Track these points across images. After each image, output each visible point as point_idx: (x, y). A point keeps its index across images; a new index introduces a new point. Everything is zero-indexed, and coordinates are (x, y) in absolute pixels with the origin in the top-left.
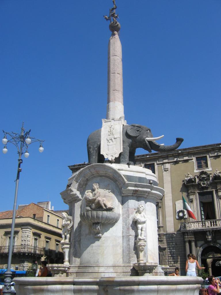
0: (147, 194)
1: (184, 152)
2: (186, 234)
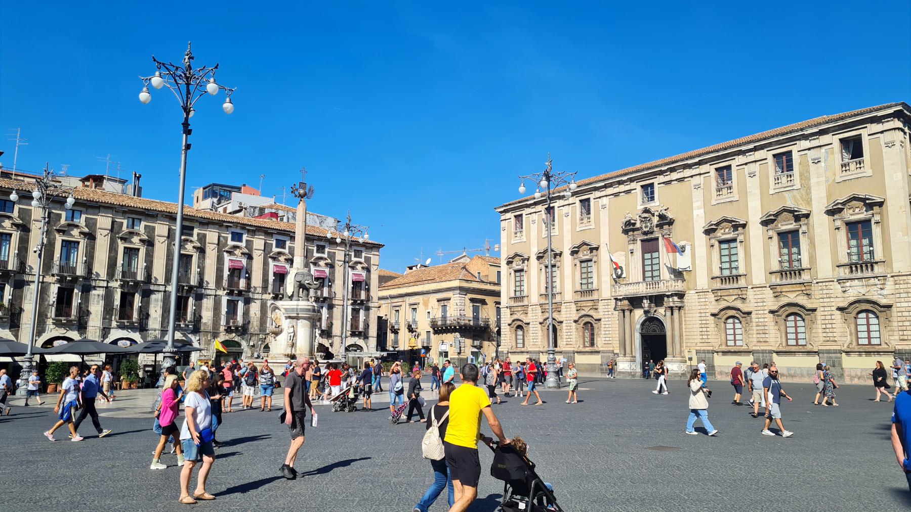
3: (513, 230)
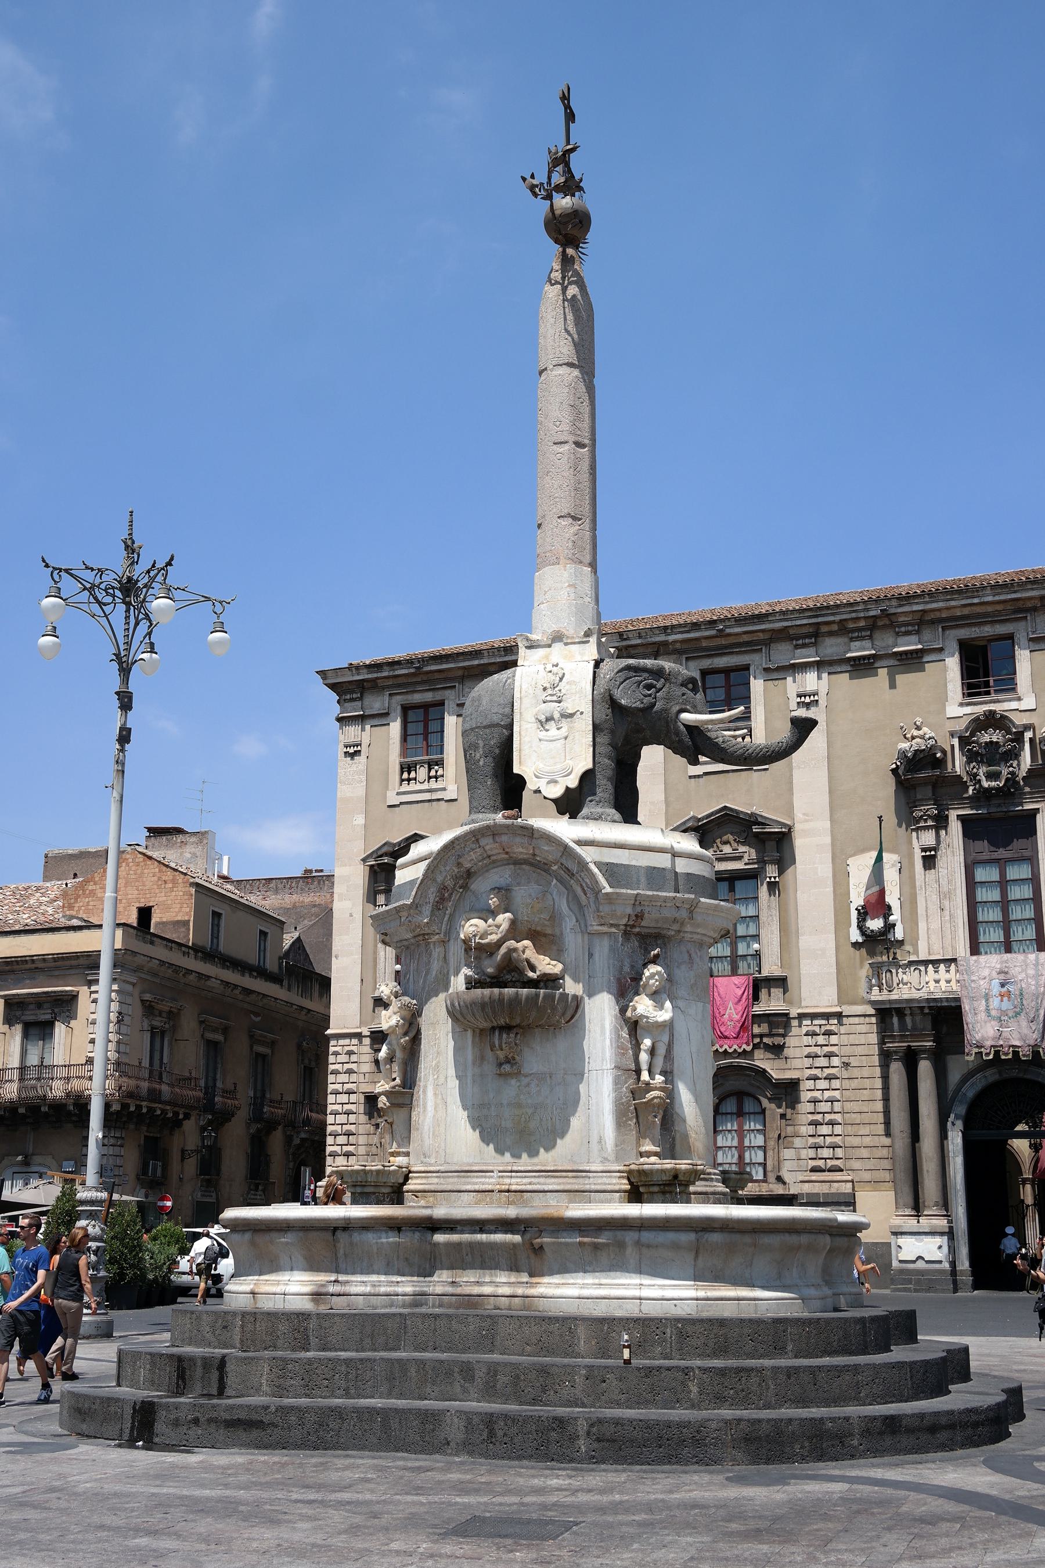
0: (676, 927)
1: (900, 610)
2: (895, 1020)
3: (395, 758)
